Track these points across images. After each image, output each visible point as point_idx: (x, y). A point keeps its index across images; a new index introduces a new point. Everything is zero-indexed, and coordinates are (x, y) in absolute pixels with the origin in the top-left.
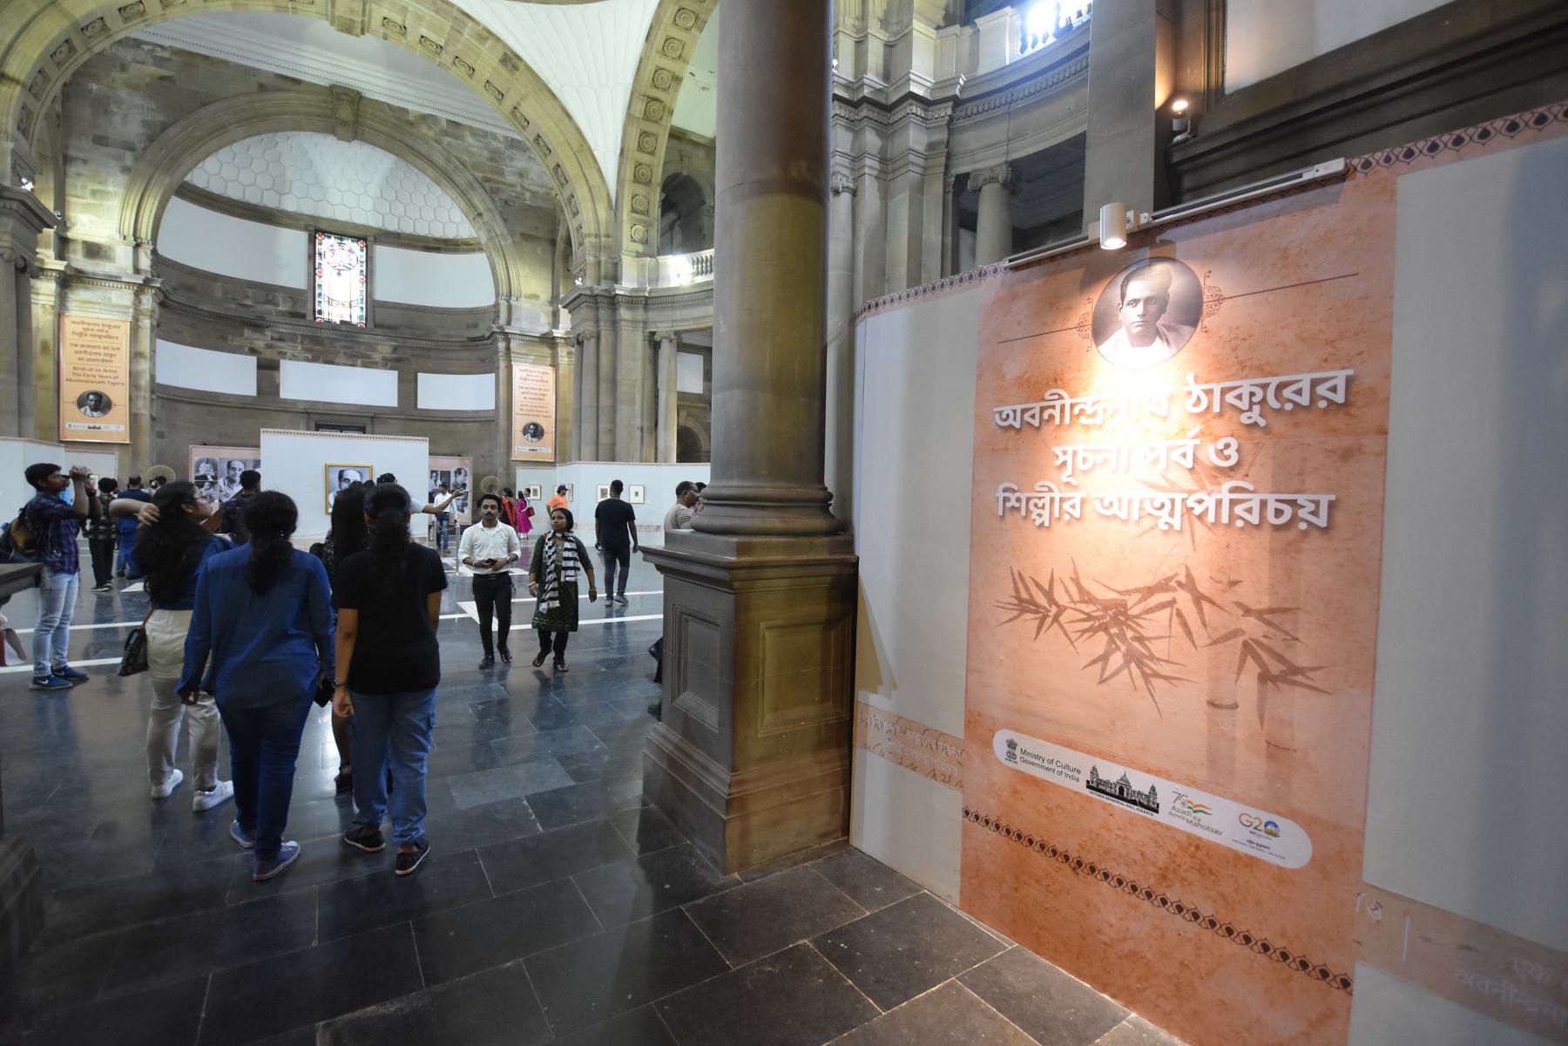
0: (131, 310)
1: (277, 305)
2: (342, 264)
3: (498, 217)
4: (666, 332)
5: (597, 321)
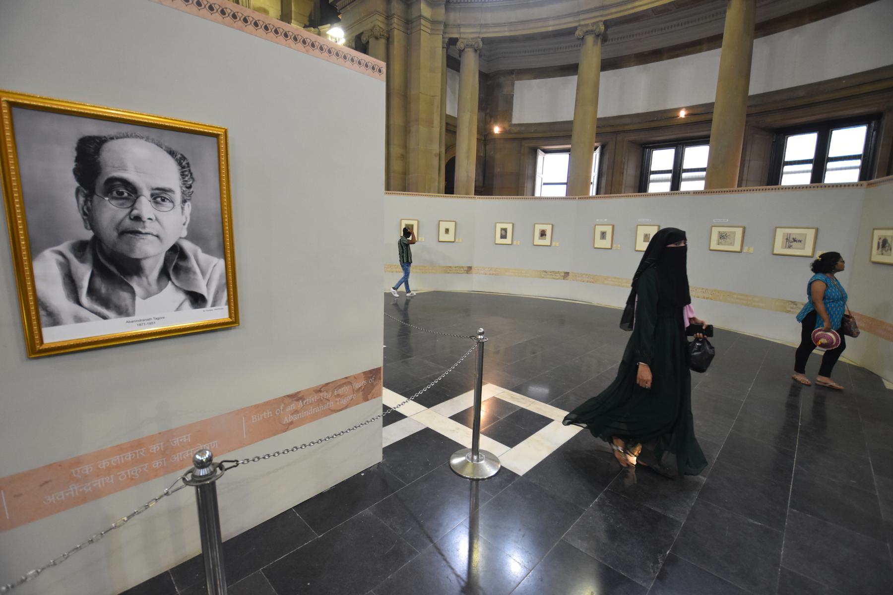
4: (473, 39)
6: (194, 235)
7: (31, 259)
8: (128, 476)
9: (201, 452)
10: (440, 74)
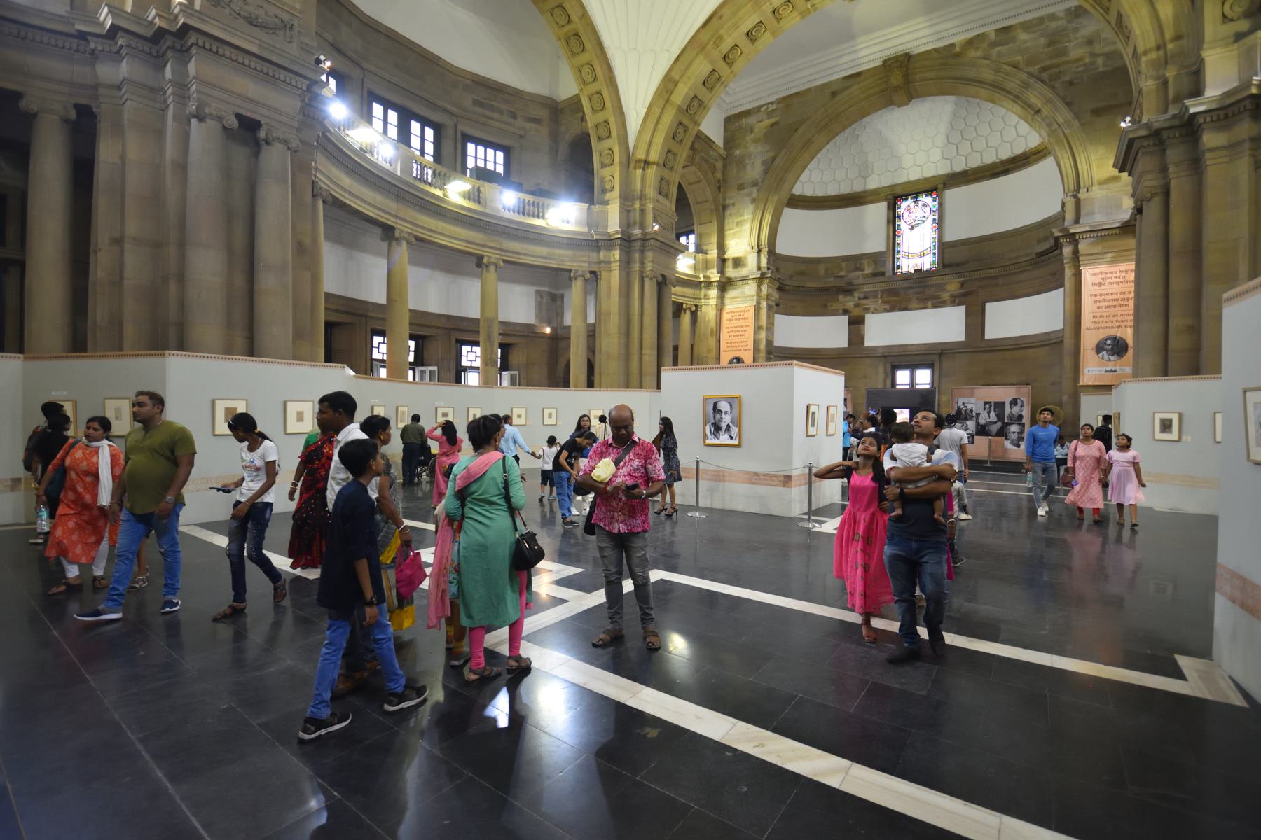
0: (755, 298)
1: (863, 270)
2: (917, 219)
3: (1060, 104)
5: (1164, 170)
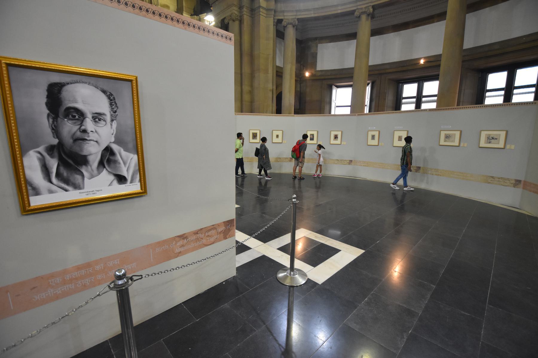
4: (291, 19)
6: (119, 141)
7: (22, 156)
8: (82, 284)
9: (119, 271)
10: (272, 41)
